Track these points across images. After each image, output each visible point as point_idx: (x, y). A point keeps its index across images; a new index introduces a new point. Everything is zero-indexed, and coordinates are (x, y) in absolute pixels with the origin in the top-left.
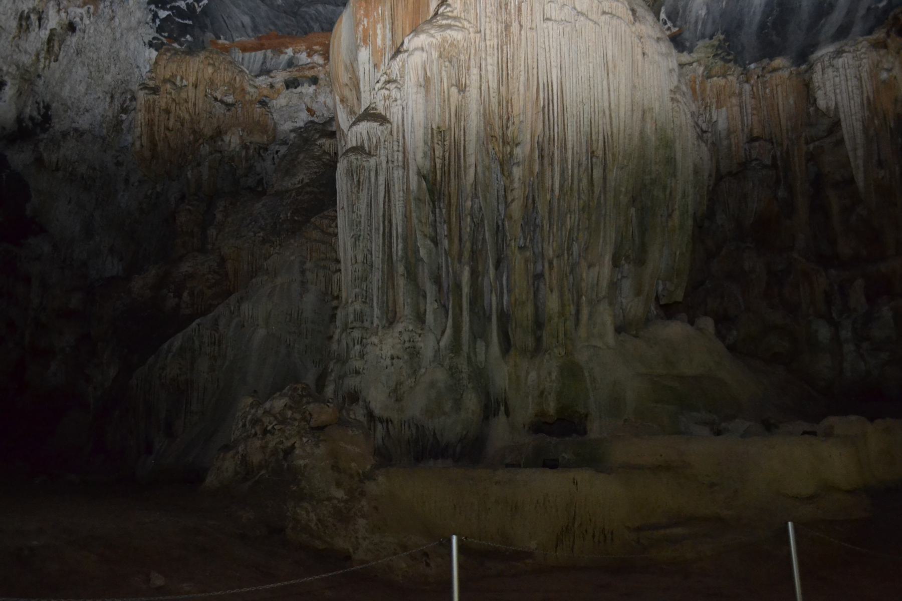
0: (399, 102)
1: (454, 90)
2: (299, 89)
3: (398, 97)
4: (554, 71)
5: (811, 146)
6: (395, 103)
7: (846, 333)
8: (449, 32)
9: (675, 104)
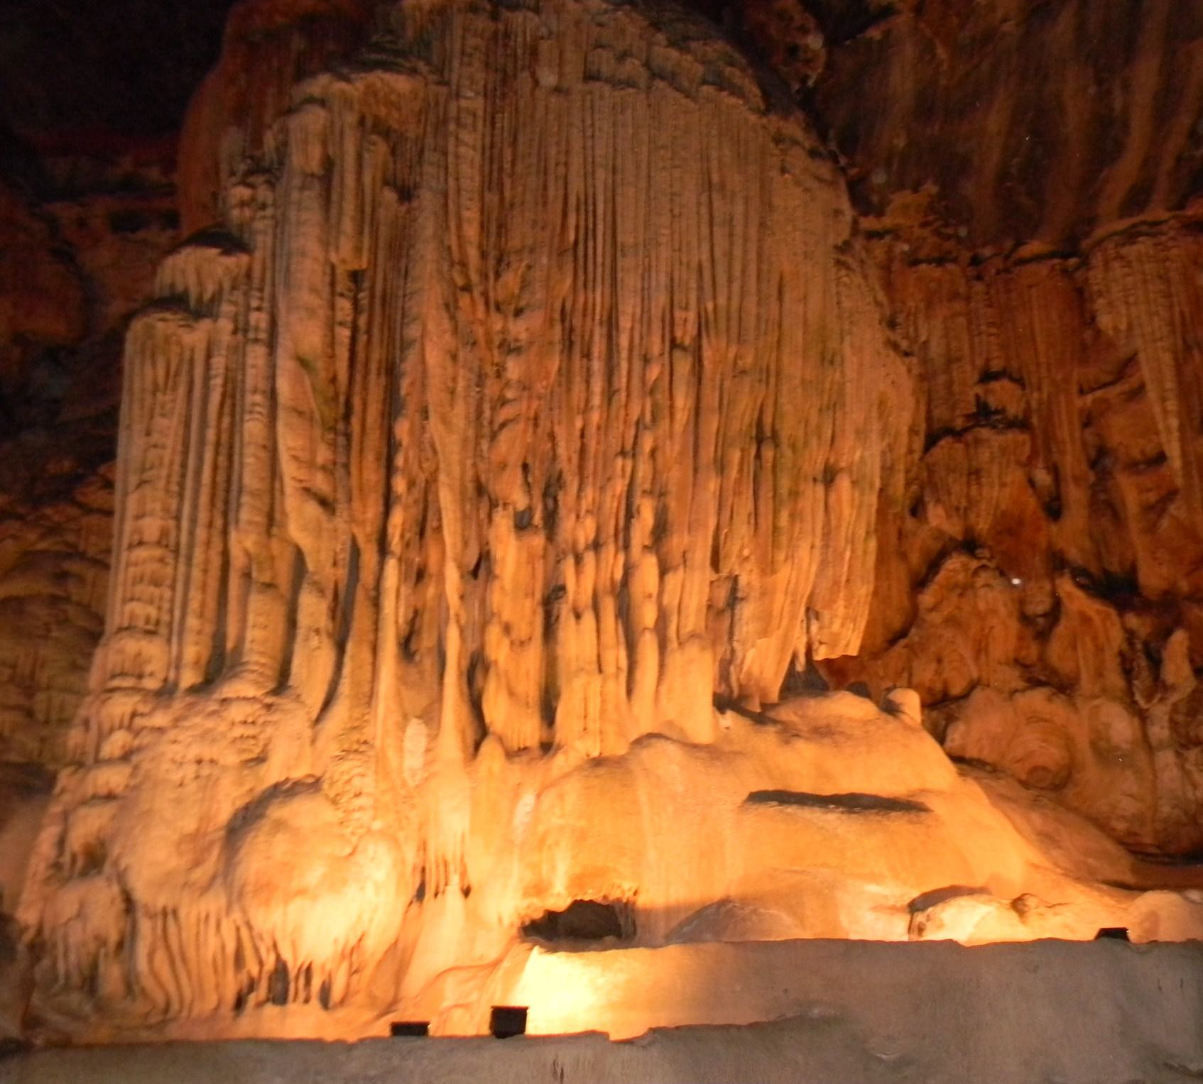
1: (390, 196)
2: (141, 234)
3: (270, 201)
5: (1089, 398)
6: (261, 213)
8: (379, 73)
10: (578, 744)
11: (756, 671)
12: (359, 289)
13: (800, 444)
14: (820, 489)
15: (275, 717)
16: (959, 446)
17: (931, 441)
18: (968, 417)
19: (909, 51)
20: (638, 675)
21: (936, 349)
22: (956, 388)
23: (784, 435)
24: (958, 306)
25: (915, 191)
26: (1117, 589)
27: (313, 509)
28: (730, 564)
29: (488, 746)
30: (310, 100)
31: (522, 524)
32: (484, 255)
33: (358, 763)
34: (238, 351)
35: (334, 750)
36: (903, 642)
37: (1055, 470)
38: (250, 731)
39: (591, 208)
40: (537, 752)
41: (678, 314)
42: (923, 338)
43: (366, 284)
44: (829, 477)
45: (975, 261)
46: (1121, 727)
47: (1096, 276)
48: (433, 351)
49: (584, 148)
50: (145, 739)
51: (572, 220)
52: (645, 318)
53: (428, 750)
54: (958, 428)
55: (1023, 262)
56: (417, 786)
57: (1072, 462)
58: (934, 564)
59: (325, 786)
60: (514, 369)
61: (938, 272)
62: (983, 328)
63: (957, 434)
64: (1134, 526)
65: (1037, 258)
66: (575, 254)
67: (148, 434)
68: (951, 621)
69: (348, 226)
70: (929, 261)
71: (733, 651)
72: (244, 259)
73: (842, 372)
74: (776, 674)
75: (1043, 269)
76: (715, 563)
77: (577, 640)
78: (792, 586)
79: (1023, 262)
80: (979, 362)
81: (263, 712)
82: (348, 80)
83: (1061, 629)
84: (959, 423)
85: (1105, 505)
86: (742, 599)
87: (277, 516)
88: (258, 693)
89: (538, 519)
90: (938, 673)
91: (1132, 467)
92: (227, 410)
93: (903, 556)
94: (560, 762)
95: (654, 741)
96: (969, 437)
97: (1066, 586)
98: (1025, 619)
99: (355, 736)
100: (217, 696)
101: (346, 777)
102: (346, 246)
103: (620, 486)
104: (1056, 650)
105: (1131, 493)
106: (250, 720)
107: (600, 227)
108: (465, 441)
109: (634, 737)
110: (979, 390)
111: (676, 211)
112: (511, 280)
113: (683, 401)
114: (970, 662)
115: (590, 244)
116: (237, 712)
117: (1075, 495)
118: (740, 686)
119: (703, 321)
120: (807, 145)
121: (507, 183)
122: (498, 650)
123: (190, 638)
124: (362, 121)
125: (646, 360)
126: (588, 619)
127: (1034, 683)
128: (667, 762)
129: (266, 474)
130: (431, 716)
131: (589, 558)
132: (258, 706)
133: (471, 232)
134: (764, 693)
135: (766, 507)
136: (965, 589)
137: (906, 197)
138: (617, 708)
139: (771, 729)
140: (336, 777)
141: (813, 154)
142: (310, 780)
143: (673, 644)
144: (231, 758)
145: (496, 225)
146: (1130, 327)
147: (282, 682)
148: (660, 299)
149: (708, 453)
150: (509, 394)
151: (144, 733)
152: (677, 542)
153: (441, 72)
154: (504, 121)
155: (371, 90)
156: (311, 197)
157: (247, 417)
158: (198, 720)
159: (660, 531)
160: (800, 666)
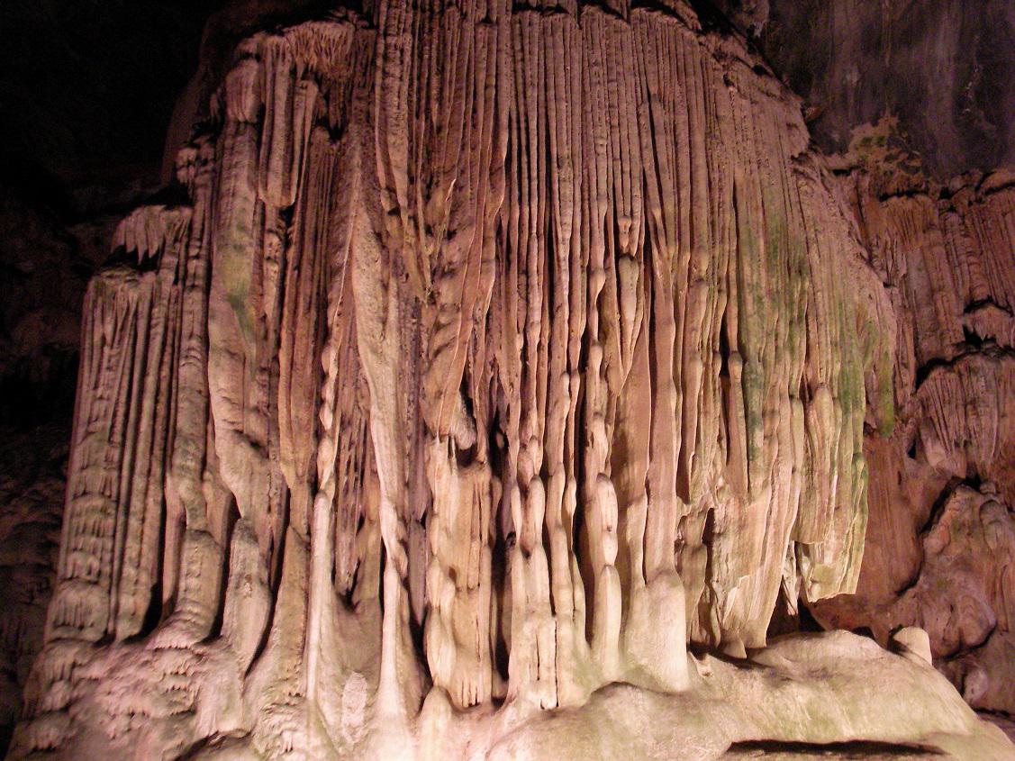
0: (209, 167)
1: (322, 135)
4: (532, 93)
9: (802, 181)
10: (530, 694)
11: (740, 614)
12: (289, 224)
13: (771, 358)
14: (798, 409)
15: (205, 668)
16: (953, 376)
17: (922, 375)
18: (958, 346)
20: (599, 617)
21: (917, 283)
22: (942, 318)
23: (754, 346)
24: (935, 235)
25: (875, 124)
27: (244, 453)
28: (700, 495)
29: (435, 703)
30: (247, 56)
31: (466, 459)
32: (412, 180)
33: (289, 718)
34: (179, 300)
35: (264, 701)
36: (911, 592)
38: (182, 684)
39: (523, 125)
40: (490, 708)
41: (624, 224)
42: (903, 271)
43: (297, 219)
44: (807, 394)
45: (946, 194)
48: (363, 279)
49: (515, 71)
50: (81, 691)
51: (504, 138)
52: (586, 229)
53: (368, 706)
54: (949, 359)
55: (991, 191)
56: (356, 745)
58: (938, 505)
59: (256, 741)
60: (447, 293)
61: (908, 204)
62: (963, 258)
63: (948, 364)
66: (511, 169)
67: (96, 387)
68: (964, 564)
69: (277, 162)
70: (899, 195)
71: (713, 593)
72: (187, 212)
73: (811, 281)
74: (762, 614)
76: (683, 492)
77: (529, 579)
78: (774, 515)
79: (991, 191)
80: (963, 292)
81: (194, 662)
82: (282, 34)
84: (949, 353)
86: (719, 534)
87: (210, 460)
88: (191, 643)
89: (483, 454)
90: (951, 622)
92: (167, 359)
93: (905, 500)
94: (509, 713)
95: (619, 690)
96: (961, 366)
99: (287, 688)
100: (149, 647)
101: (277, 732)
102: (275, 183)
103: (567, 407)
106: (182, 671)
107: (534, 142)
108: (400, 374)
109: (597, 686)
110: (967, 320)
111: (615, 122)
112: (440, 199)
113: (633, 314)
114: (985, 606)
115: (524, 159)
116: (168, 663)
118: (723, 631)
119: (652, 229)
120: (752, 64)
121: (435, 107)
122: (441, 594)
123: (127, 586)
124: (293, 72)
125: (590, 272)
126: (539, 556)
128: (632, 711)
129: (200, 420)
130: (370, 670)
131: (537, 490)
132: (189, 656)
133: (399, 157)
134: (750, 637)
135: (739, 427)
136: (973, 529)
137: (868, 130)
138: (575, 654)
139: (756, 673)
140: (266, 731)
141: (758, 71)
142: (240, 735)
143: (640, 583)
144: (161, 712)
145: (425, 151)
147: (214, 633)
148: (602, 209)
149: (667, 370)
150: (443, 320)
151: (82, 684)
152: (637, 472)
154: (432, 53)
155: (303, 43)
156: (244, 144)
157: (182, 362)
158: (131, 670)
159: (620, 459)
160: (793, 608)
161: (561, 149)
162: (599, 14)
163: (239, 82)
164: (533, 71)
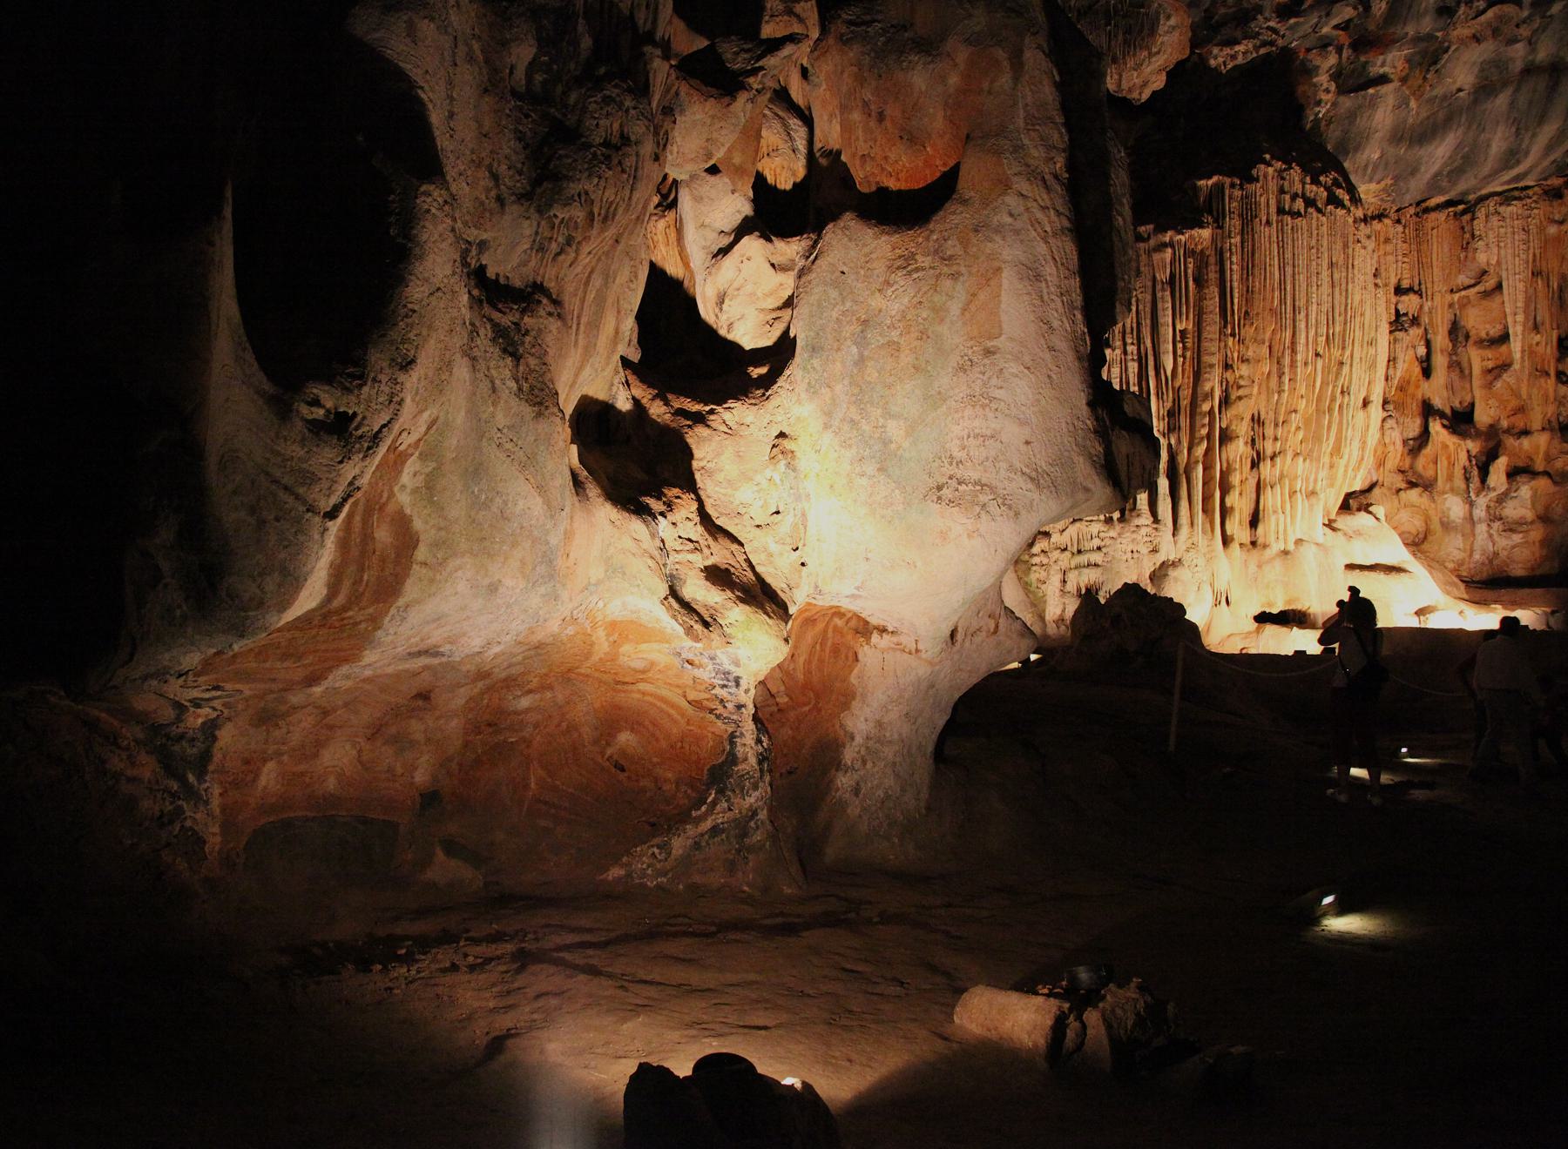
4: (1289, 270)
5: (1456, 296)
7: (1480, 512)
19: (1391, 101)
26: (1461, 421)
30: (1165, 245)
37: (1428, 344)
46: (1455, 508)
47: (1479, 225)
55: (1427, 210)
57: (1441, 340)
64: (1476, 382)
65: (1438, 207)
75: (1441, 216)
83: (1428, 451)
85: (1456, 366)
91: (1480, 343)
97: (1436, 427)
98: (1405, 442)
104: (1422, 462)
105: (1477, 359)
117: (1440, 361)
127: (1412, 485)
131: (1278, 460)
146: (1499, 263)
147: (1156, 520)
150: (1242, 383)
153: (1219, 224)
161: (1301, 303)
162: (1315, 214)
163: (1163, 260)
164: (1288, 255)
